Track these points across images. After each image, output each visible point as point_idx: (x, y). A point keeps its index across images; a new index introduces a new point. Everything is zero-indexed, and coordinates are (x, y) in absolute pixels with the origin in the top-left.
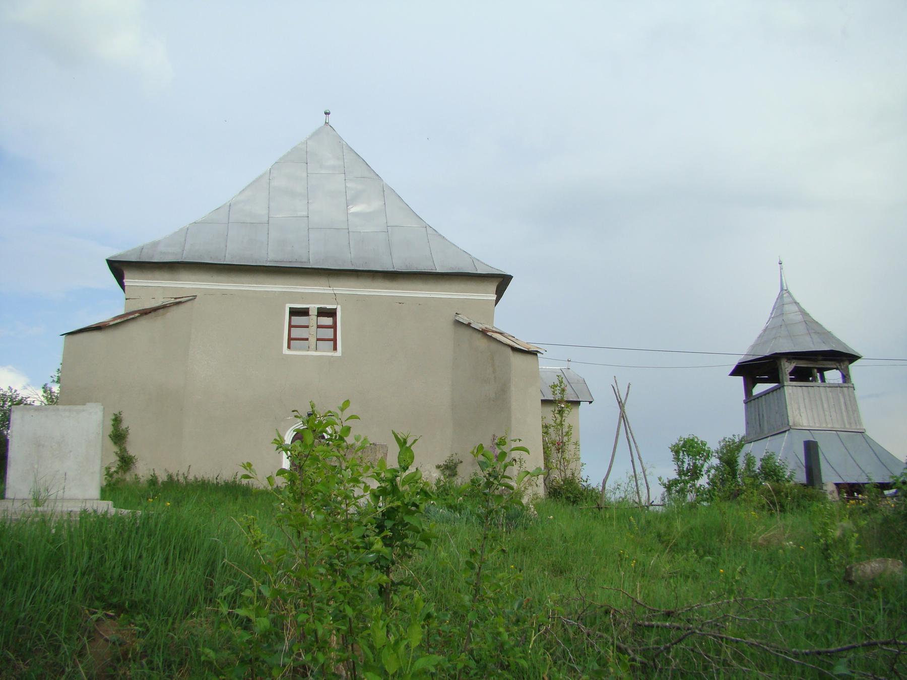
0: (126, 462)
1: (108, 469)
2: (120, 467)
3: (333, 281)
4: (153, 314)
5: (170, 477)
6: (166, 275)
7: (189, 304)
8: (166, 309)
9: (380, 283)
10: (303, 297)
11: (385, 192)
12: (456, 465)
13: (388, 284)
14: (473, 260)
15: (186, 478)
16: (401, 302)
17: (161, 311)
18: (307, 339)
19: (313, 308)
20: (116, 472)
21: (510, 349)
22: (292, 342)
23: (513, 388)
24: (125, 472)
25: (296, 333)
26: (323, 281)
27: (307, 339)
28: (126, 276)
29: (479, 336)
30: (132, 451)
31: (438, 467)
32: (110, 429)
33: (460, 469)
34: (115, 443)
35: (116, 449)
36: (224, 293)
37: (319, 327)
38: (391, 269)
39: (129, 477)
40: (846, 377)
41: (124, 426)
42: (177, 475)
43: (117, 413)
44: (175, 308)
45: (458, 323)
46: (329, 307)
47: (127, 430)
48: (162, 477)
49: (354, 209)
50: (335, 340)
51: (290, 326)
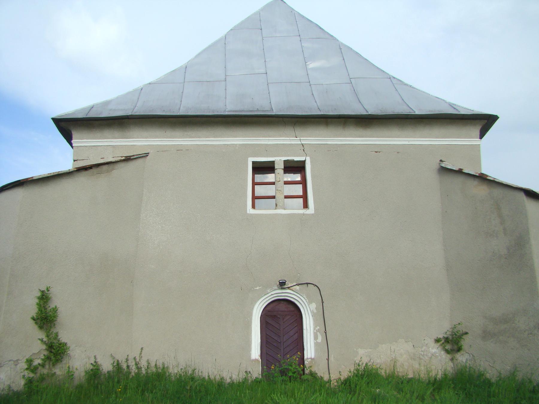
0: (56, 351)
1: (30, 362)
2: (48, 358)
3: (299, 131)
4: (94, 170)
5: (118, 366)
6: (116, 133)
7: (140, 161)
8: (111, 166)
10: (266, 149)
11: (342, 49)
12: (460, 337)
13: (361, 131)
14: (451, 105)
15: (136, 364)
16: (378, 150)
17: (105, 167)
18: (274, 197)
19: (279, 161)
20: (43, 366)
21: (522, 195)
22: (256, 201)
23: (533, 242)
24: (54, 365)
25: (260, 191)
26: (289, 130)
27: (274, 197)
28: (74, 136)
29: (475, 182)
30: (65, 336)
31: (437, 341)
32: (33, 311)
33: (466, 342)
34: (41, 328)
35: (42, 335)
36: (179, 149)
37: (286, 183)
38: (365, 113)
39: (59, 371)
41: (52, 305)
42: (127, 360)
43: (44, 289)
44: (122, 165)
45: (444, 170)
46: (297, 159)
47: (55, 310)
48: (107, 366)
49: (312, 65)
50: (305, 197)
51: (254, 184)
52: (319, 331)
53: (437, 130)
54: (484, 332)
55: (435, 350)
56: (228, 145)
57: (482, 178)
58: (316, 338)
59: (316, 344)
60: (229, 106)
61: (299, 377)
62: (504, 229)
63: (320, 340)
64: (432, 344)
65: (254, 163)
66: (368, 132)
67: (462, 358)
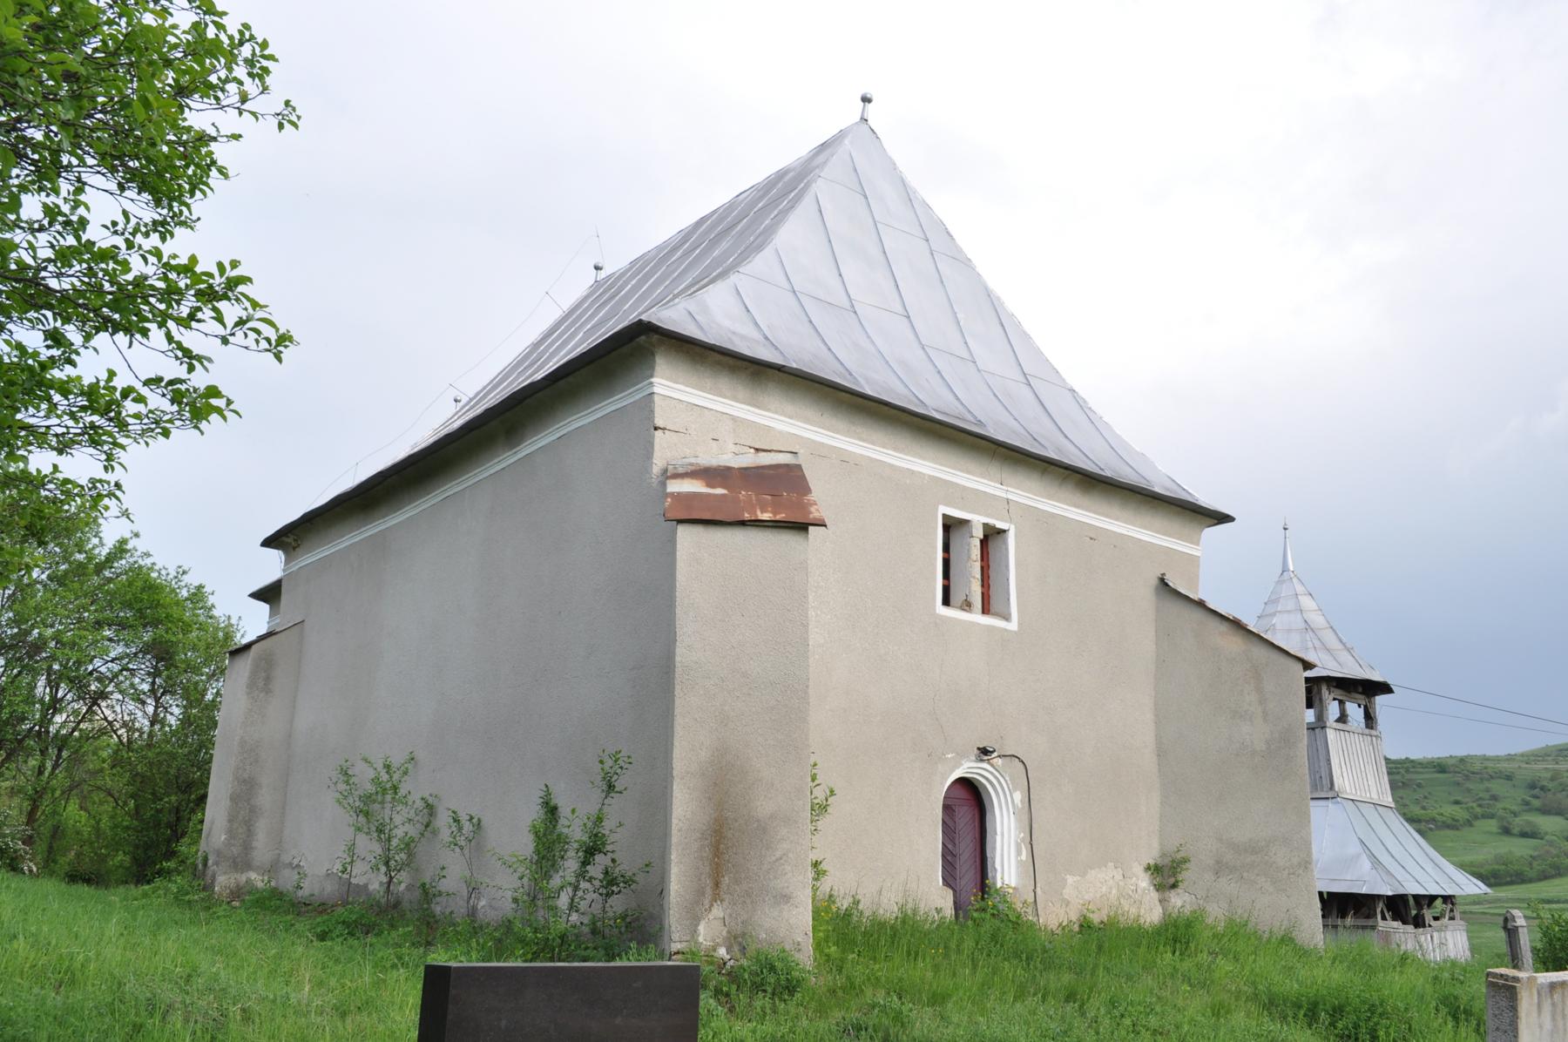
3: (1007, 473)
6: (742, 391)
9: (1069, 492)
13: (1078, 497)
16: (1095, 535)
19: (978, 520)
26: (994, 468)
29: (1224, 627)
31: (1148, 868)
33: (1185, 875)
40: (1370, 719)
52: (1023, 840)
53: (1160, 520)
54: (1218, 862)
55: (1144, 882)
56: (913, 472)
57: (1237, 624)
58: (1019, 853)
59: (1020, 863)
60: (933, 400)
61: (997, 922)
62: (1265, 714)
63: (1024, 857)
64: (1138, 870)
65: (945, 516)
66: (1085, 500)
67: (1177, 900)
